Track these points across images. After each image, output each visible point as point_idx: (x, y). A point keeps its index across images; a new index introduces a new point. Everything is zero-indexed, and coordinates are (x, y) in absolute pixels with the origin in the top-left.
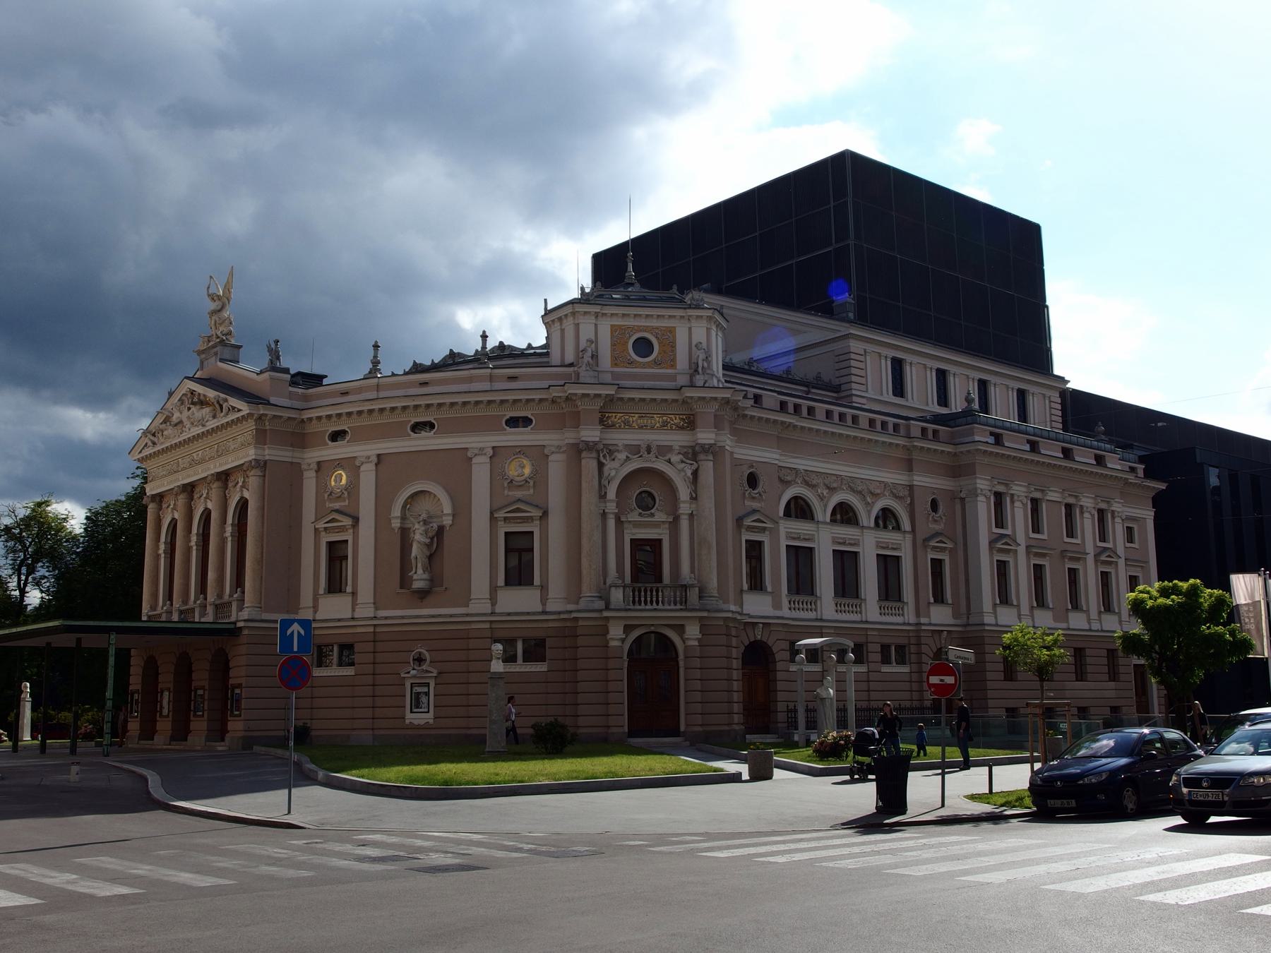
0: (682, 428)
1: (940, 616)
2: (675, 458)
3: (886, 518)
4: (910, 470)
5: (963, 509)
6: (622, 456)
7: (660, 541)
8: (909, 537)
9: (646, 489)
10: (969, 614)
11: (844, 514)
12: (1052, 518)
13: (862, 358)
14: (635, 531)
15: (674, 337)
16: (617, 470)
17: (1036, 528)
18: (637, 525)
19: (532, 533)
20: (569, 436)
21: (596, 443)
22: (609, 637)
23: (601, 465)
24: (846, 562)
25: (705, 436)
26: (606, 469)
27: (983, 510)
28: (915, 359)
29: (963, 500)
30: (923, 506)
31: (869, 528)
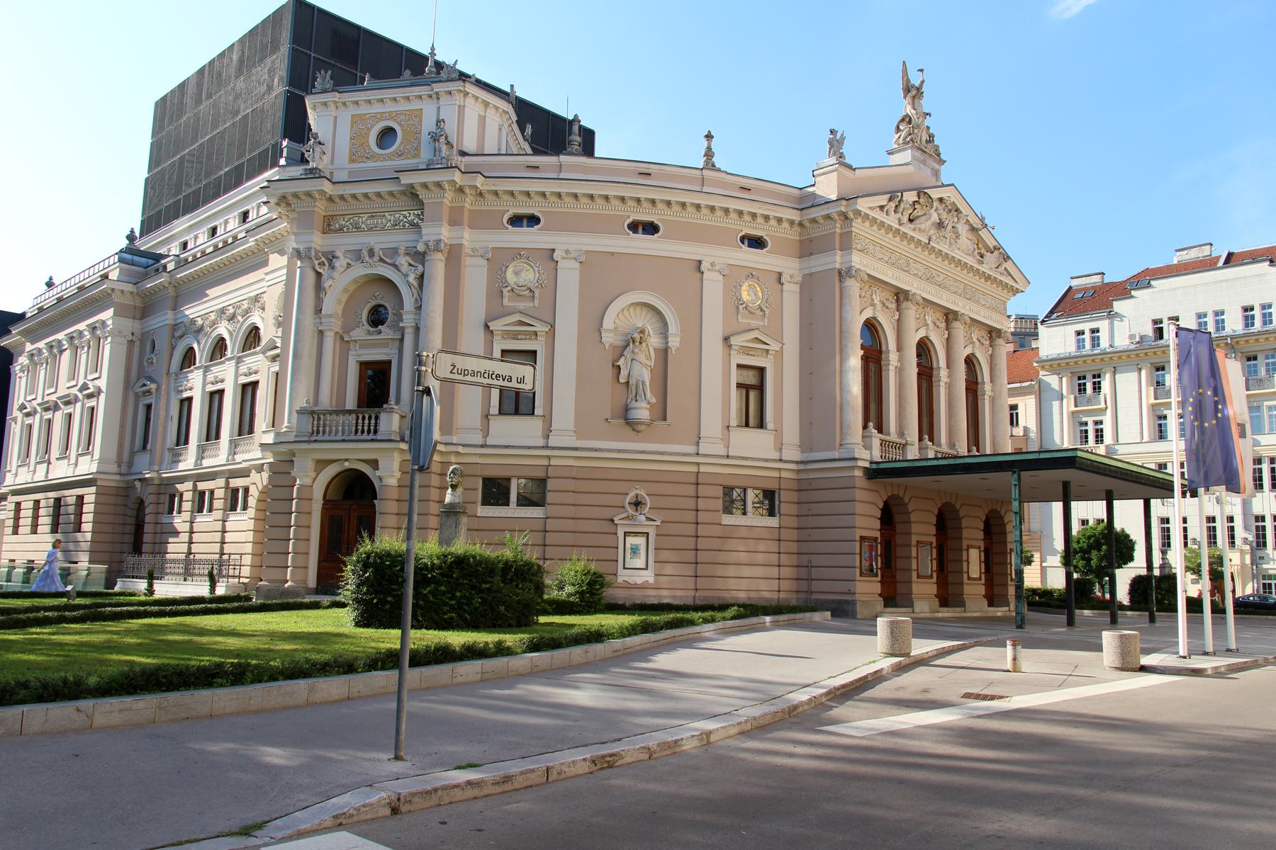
2: (403, 261)
7: (389, 362)
23: (319, 275)
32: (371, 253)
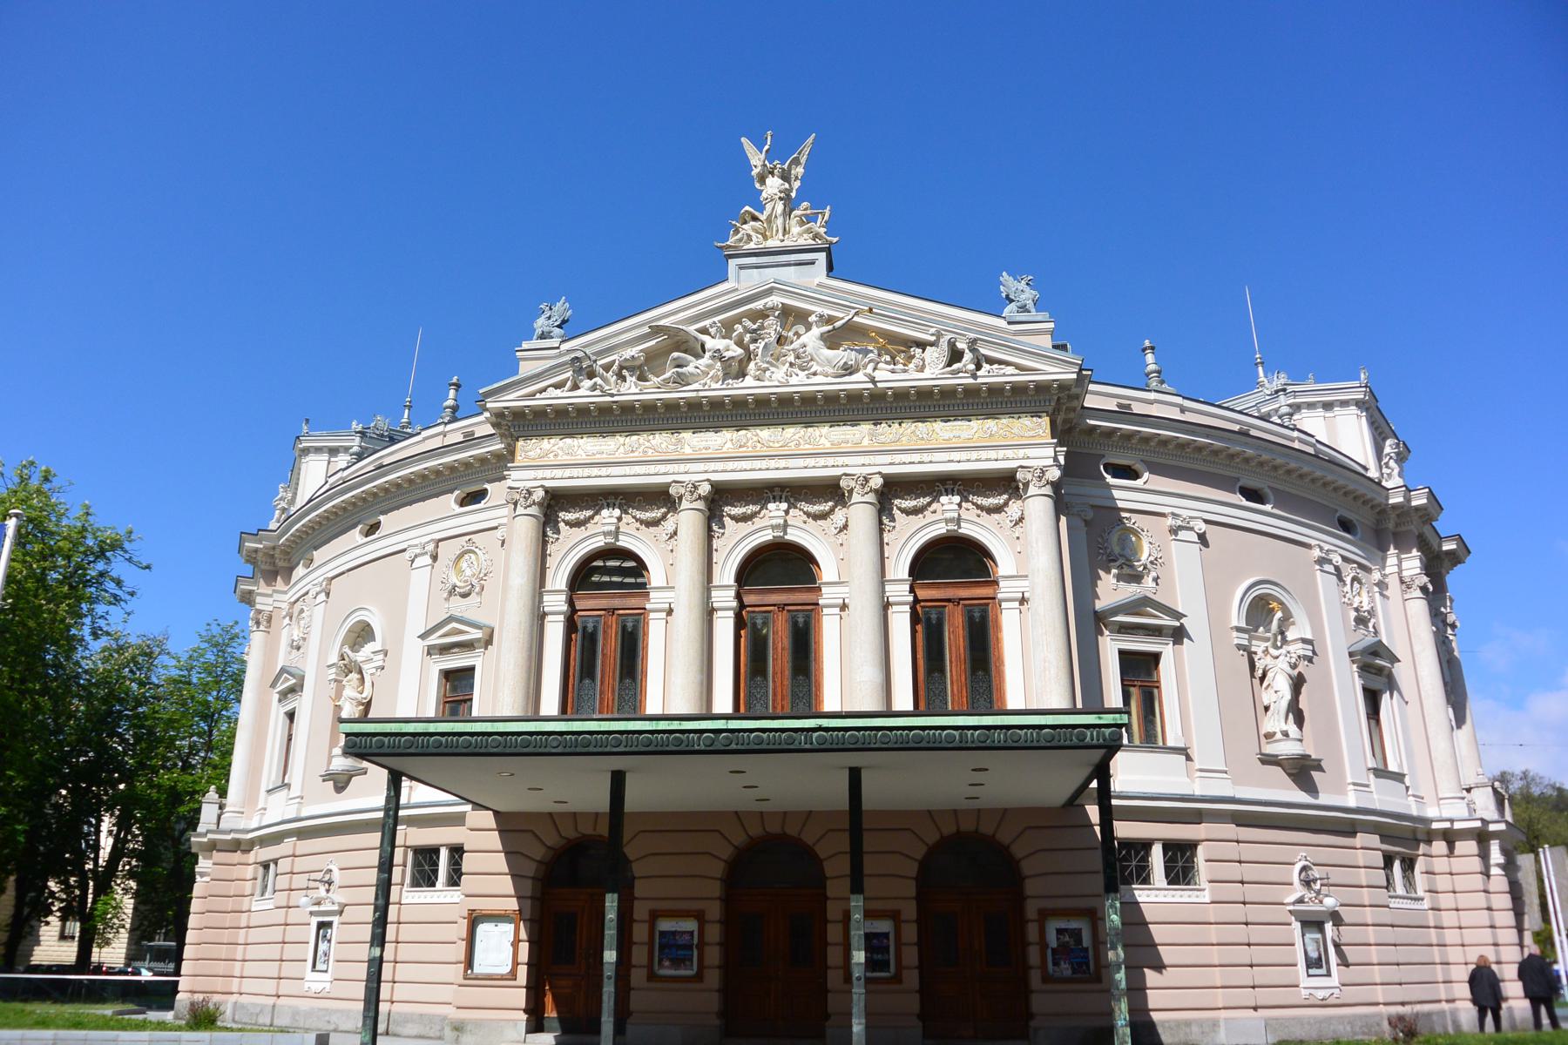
19: (472, 669)
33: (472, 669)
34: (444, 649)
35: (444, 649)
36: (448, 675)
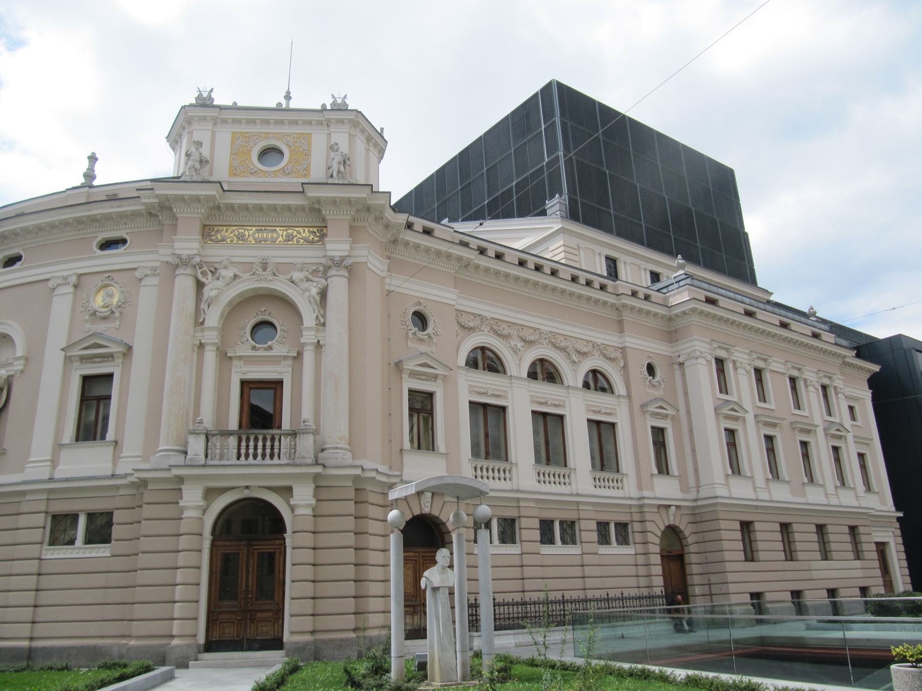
0: (312, 242)
1: (666, 489)
3: (596, 381)
4: (621, 331)
5: (683, 375)
6: (228, 273)
8: (624, 402)
9: (264, 316)
10: (698, 487)
11: (543, 371)
12: (777, 387)
13: (575, 252)
14: (246, 369)
15: (309, 144)
16: (222, 292)
17: (763, 398)
18: (248, 360)
19: (110, 376)
20: (164, 254)
21: (191, 257)
22: (181, 504)
23: (200, 285)
24: (549, 424)
25: (337, 247)
26: (206, 290)
27: (703, 376)
28: (630, 260)
29: (681, 364)
30: (638, 371)
31: (576, 388)
32: (264, 266)
33: (110, 376)
34: (83, 359)
35: (83, 359)
36: (86, 379)
